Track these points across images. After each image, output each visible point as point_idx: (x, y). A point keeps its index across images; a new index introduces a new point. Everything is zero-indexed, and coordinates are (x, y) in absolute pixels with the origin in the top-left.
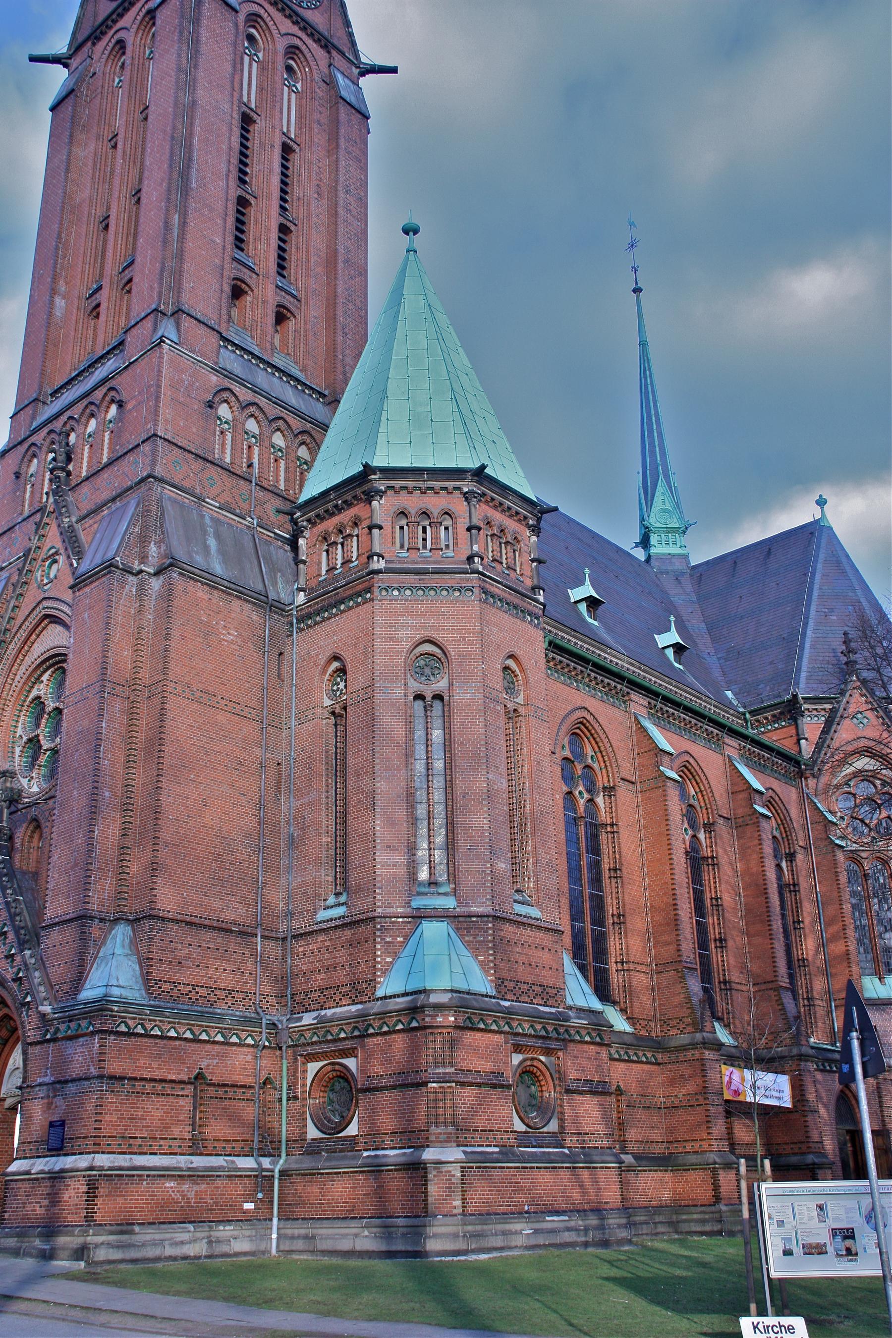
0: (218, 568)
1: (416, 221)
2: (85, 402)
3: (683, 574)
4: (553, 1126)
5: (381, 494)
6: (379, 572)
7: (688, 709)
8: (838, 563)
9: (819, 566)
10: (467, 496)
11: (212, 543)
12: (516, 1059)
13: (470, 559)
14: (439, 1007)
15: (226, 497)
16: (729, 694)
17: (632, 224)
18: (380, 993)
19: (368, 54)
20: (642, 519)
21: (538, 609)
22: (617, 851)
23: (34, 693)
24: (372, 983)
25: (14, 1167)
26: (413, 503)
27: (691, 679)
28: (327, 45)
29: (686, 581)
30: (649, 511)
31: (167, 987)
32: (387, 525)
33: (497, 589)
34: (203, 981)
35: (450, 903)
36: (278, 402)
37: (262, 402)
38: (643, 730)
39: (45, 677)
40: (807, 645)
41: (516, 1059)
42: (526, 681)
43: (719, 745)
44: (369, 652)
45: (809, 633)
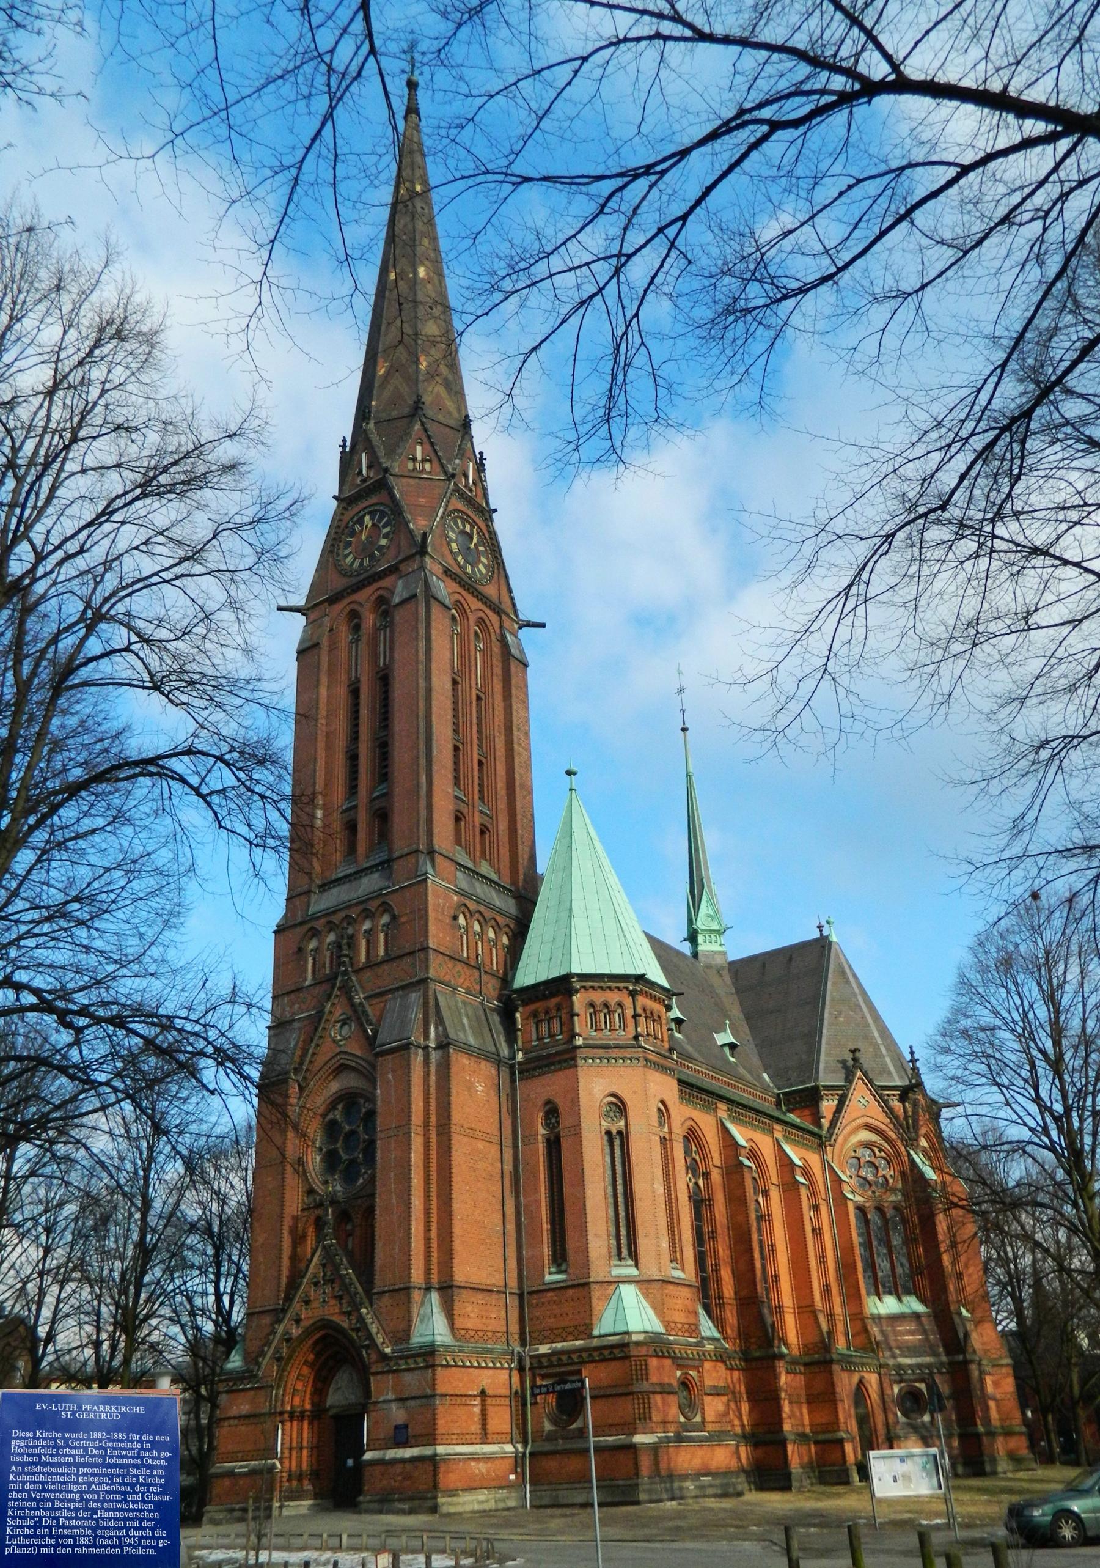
0: (472, 1041)
1: (574, 768)
2: (361, 907)
3: (723, 968)
4: (698, 1419)
5: (577, 991)
6: (580, 1047)
7: (752, 1109)
8: (843, 973)
9: (830, 976)
10: (633, 994)
11: (465, 1021)
12: (679, 1373)
13: (636, 1038)
14: (638, 1344)
15: (467, 984)
16: (765, 1076)
17: (680, 672)
18: (596, 1332)
19: (525, 614)
20: (690, 922)
21: (671, 1064)
22: (713, 1218)
23: (330, 1116)
24: (589, 1327)
25: (368, 1456)
26: (598, 997)
27: (742, 1071)
28: (498, 611)
29: (725, 973)
30: (697, 916)
31: (463, 1332)
32: (582, 1013)
33: (652, 1057)
34: (480, 1327)
35: (633, 1271)
36: (490, 906)
37: (482, 909)
38: (726, 1130)
39: (340, 1107)
40: (824, 1042)
41: (679, 1373)
42: (669, 1117)
43: (771, 1131)
44: (575, 1101)
45: (825, 1031)
